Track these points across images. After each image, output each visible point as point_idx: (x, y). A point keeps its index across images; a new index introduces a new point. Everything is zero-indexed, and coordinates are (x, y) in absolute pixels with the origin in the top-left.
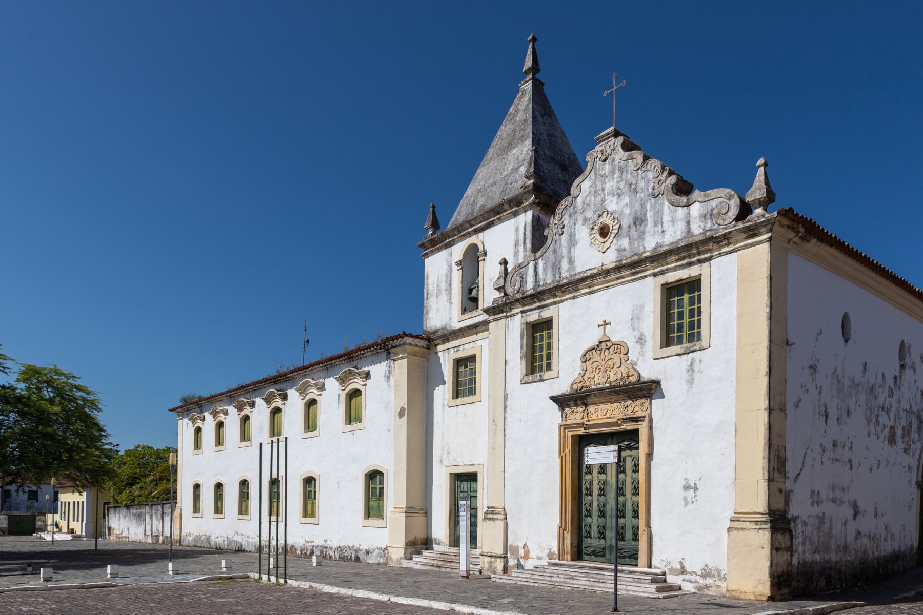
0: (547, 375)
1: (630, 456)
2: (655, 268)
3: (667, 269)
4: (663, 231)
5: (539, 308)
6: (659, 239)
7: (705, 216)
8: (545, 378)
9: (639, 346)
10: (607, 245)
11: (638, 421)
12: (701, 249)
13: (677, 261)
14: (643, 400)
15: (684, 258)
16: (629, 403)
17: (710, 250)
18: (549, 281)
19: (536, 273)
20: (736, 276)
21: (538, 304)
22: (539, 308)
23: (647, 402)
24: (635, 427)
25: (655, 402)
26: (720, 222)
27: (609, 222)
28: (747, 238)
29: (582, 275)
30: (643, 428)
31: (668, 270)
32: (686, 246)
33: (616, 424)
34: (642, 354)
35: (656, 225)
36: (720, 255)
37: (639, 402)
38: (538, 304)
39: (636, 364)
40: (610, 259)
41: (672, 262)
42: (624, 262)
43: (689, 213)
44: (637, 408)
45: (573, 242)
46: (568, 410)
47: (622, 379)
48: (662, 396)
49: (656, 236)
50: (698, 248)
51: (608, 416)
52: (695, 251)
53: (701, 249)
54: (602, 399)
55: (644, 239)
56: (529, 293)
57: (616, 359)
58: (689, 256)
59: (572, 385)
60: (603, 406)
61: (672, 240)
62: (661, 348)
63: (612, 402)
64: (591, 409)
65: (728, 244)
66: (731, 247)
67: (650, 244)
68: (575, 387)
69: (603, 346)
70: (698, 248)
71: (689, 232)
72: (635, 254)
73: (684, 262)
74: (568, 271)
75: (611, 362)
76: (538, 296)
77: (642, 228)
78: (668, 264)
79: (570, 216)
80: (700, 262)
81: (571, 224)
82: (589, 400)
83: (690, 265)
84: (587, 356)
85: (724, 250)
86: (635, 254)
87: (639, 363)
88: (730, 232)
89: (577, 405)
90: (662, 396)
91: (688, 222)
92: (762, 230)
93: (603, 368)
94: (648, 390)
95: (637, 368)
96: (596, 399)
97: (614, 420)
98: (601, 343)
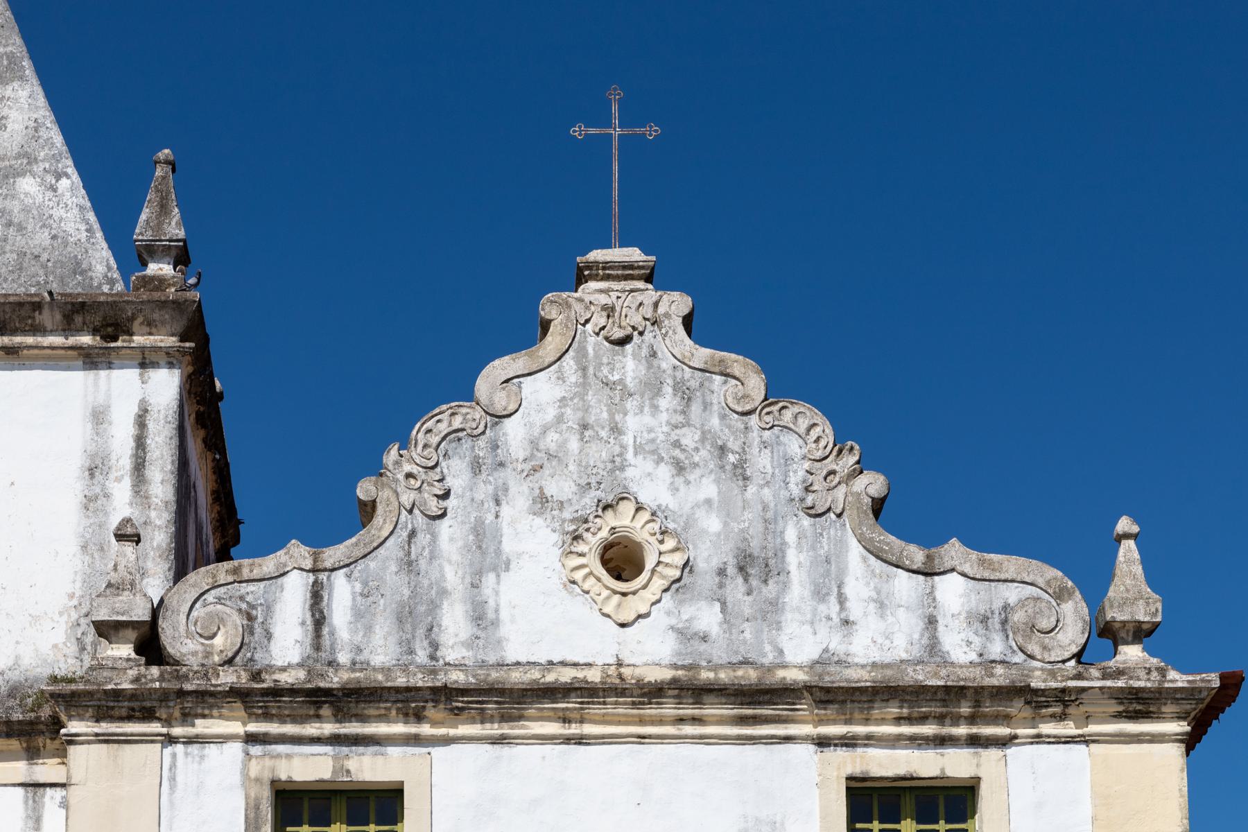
2: (821, 722)
3: (869, 737)
4: (846, 622)
5: (335, 740)
6: (836, 644)
7: (984, 620)
10: (638, 604)
12: (987, 710)
13: (899, 720)
15: (923, 719)
17: (1006, 719)
18: (378, 660)
19: (319, 620)
20: (1087, 810)
21: (328, 728)
22: (335, 740)
26: (1034, 648)
27: (640, 530)
28: (1118, 716)
29: (535, 674)
31: (870, 740)
32: (947, 689)
35: (820, 594)
36: (1038, 739)
38: (328, 728)
40: (651, 651)
41: (882, 721)
42: (706, 675)
43: (931, 593)
45: (486, 555)
49: (823, 629)
50: (977, 704)
52: (965, 710)
53: (987, 710)
55: (778, 626)
56: (287, 679)
58: (941, 719)
61: (876, 656)
65: (1062, 717)
66: (1069, 729)
67: (798, 648)
70: (977, 704)
71: (933, 646)
72: (745, 662)
73: (928, 729)
74: (470, 644)
76: (343, 701)
77: (771, 589)
78: (867, 721)
79: (476, 467)
80: (974, 741)
81: (484, 491)
83: (942, 741)
85: (1048, 728)
86: (745, 662)
88: (1084, 690)
91: (932, 621)
92: (1169, 709)
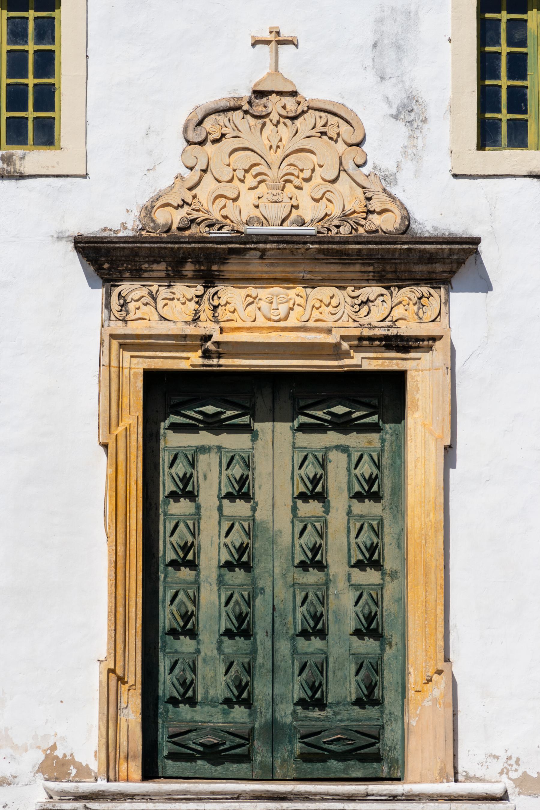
0: (33, 158)
1: (344, 449)
8: (27, 168)
9: (401, 129)
11: (406, 349)
14: (424, 289)
16: (372, 291)
23: (437, 296)
24: (394, 366)
25: (461, 301)
30: (422, 375)
33: (334, 351)
34: (412, 153)
37: (408, 293)
39: (389, 178)
44: (401, 308)
46: (131, 289)
47: (345, 217)
48: (485, 285)
51: (292, 322)
54: (278, 271)
57: (327, 154)
59: (148, 211)
60: (277, 290)
62: (478, 149)
63: (310, 283)
64: (231, 295)
68: (162, 217)
69: (274, 104)
75: (304, 161)
82: (233, 267)
84: (208, 124)
87: (405, 176)
89: (174, 275)
90: (485, 285)
93: (274, 174)
94: (446, 263)
95: (393, 191)
96: (257, 267)
97: (333, 339)
98: (259, 94)
